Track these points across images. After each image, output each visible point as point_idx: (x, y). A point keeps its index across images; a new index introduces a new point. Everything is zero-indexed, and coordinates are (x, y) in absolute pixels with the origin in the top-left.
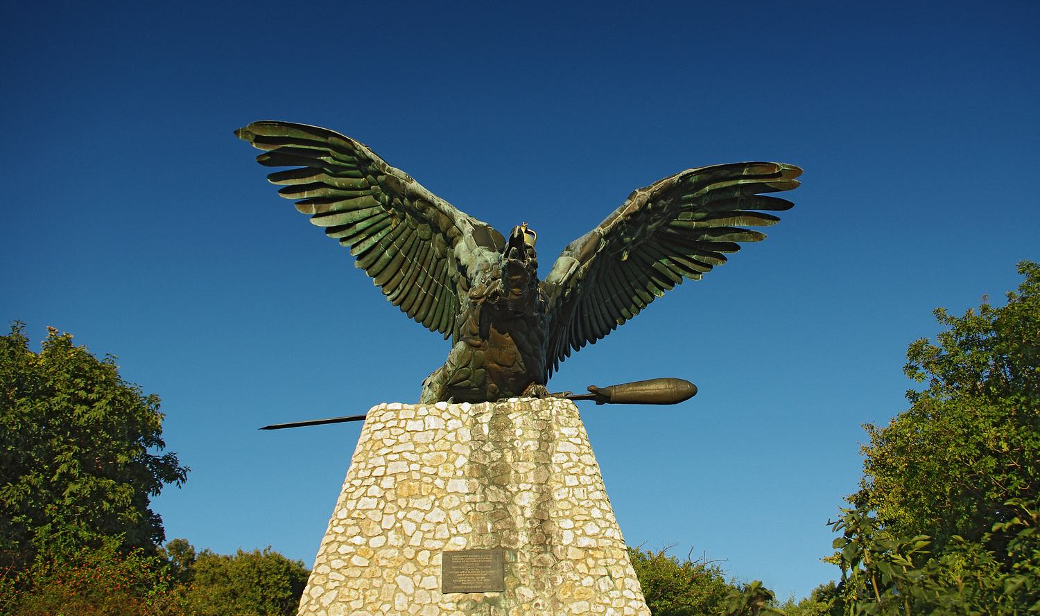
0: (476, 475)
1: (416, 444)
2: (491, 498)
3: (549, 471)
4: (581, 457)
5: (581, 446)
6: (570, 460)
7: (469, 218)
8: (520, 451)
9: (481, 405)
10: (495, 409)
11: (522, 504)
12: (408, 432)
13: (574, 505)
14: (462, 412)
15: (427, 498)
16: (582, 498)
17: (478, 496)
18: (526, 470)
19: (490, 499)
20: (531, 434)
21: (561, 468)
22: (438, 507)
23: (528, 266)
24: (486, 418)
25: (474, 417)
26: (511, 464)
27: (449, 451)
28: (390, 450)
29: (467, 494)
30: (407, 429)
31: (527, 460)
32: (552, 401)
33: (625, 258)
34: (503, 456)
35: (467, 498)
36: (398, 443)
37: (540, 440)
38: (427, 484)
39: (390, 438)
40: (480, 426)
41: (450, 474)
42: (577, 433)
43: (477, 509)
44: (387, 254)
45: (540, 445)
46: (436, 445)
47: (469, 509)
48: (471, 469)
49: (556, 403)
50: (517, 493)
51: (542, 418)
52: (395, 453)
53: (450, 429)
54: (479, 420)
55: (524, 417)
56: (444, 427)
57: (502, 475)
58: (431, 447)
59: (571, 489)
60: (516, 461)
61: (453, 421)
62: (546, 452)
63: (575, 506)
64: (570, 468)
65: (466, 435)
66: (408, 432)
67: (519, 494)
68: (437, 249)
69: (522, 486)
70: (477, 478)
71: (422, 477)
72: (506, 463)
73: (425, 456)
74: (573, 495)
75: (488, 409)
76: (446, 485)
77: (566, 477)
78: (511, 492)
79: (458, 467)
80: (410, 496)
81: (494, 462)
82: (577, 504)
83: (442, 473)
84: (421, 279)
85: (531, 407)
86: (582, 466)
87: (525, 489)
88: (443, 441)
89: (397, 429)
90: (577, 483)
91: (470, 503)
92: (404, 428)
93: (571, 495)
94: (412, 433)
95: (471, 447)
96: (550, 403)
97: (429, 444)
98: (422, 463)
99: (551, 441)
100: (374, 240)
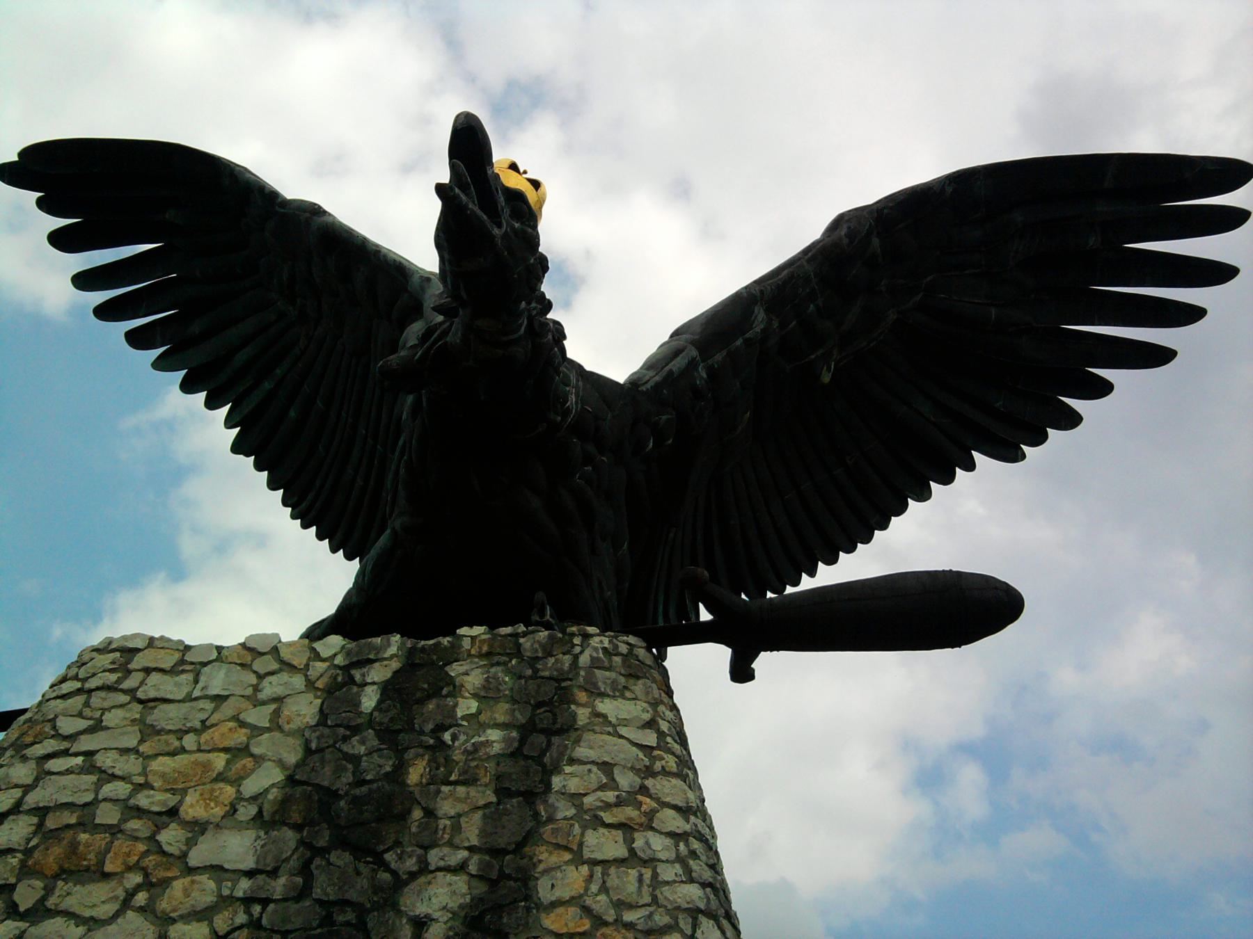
0: (296, 817)
1: (149, 731)
2: (323, 887)
3: (536, 815)
4: (649, 783)
5: (656, 753)
6: (612, 784)
8: (457, 756)
9: (378, 640)
10: (412, 652)
11: (421, 909)
12: (141, 702)
13: (599, 922)
14: (317, 656)
15: (113, 883)
16: (633, 899)
17: (282, 880)
18: (460, 808)
19: (317, 892)
20: (501, 712)
21: (580, 807)
22: (142, 910)
23: (505, 235)
24: (379, 673)
25: (346, 669)
26: (417, 791)
27: (242, 751)
28: (62, 747)
29: (250, 874)
30: (140, 694)
31: (469, 780)
32: (586, 636)
33: (826, 378)
34: (401, 768)
35: (244, 885)
36: (97, 727)
37: (527, 730)
38: (136, 839)
39: (80, 715)
40: (355, 689)
41: (219, 811)
42: (647, 717)
43: (264, 922)
44: (292, 414)
45: (523, 741)
46: (205, 737)
47: (241, 918)
48: (285, 802)
49: (595, 641)
50: (413, 876)
51: (547, 674)
52: (76, 755)
53: (262, 696)
54: (358, 677)
55: (493, 670)
56: (249, 691)
57: (380, 820)
58: (189, 741)
59: (599, 869)
60: (435, 781)
61: (284, 677)
62: (539, 759)
63: (606, 924)
64: (607, 806)
65: (305, 709)
66: (141, 702)
67: (422, 880)
69: (434, 857)
70: (298, 828)
71: (124, 820)
72: (404, 784)
73: (162, 764)
74: (604, 889)
75: (393, 650)
76: (191, 843)
77: (589, 832)
78: (394, 873)
79: (247, 794)
80: (64, 873)
81: (364, 782)
82: (610, 916)
83: (193, 807)
85: (519, 646)
86: (648, 803)
87: (442, 864)
88: (232, 724)
89: (111, 695)
90: (622, 852)
91: (247, 901)
92: (132, 692)
93: (594, 888)
94: (152, 704)
95: (307, 743)
96: (577, 641)
97: (187, 732)
98: (141, 780)
99: (561, 732)
100: (267, 385)
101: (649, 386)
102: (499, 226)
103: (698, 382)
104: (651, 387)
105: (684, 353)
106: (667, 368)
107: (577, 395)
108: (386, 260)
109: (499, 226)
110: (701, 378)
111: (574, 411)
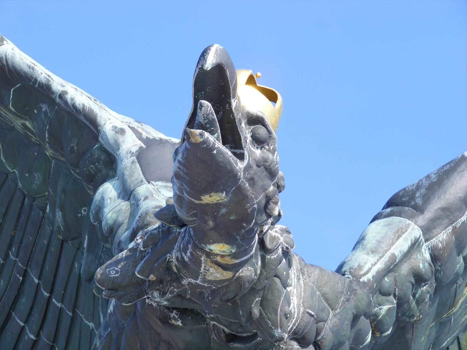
7: (135, 125)
68: (59, 214)
84: (25, 303)
101: (370, 276)
102: (241, 157)
103: (421, 266)
104: (373, 277)
105: (407, 233)
106: (388, 254)
107: (299, 297)
108: (74, 106)
109: (241, 157)
110: (424, 260)
111: (296, 316)
